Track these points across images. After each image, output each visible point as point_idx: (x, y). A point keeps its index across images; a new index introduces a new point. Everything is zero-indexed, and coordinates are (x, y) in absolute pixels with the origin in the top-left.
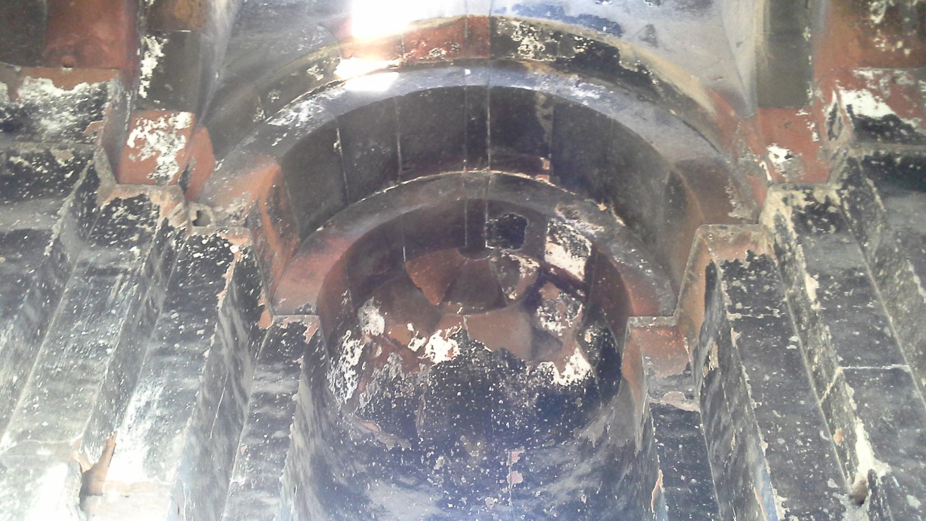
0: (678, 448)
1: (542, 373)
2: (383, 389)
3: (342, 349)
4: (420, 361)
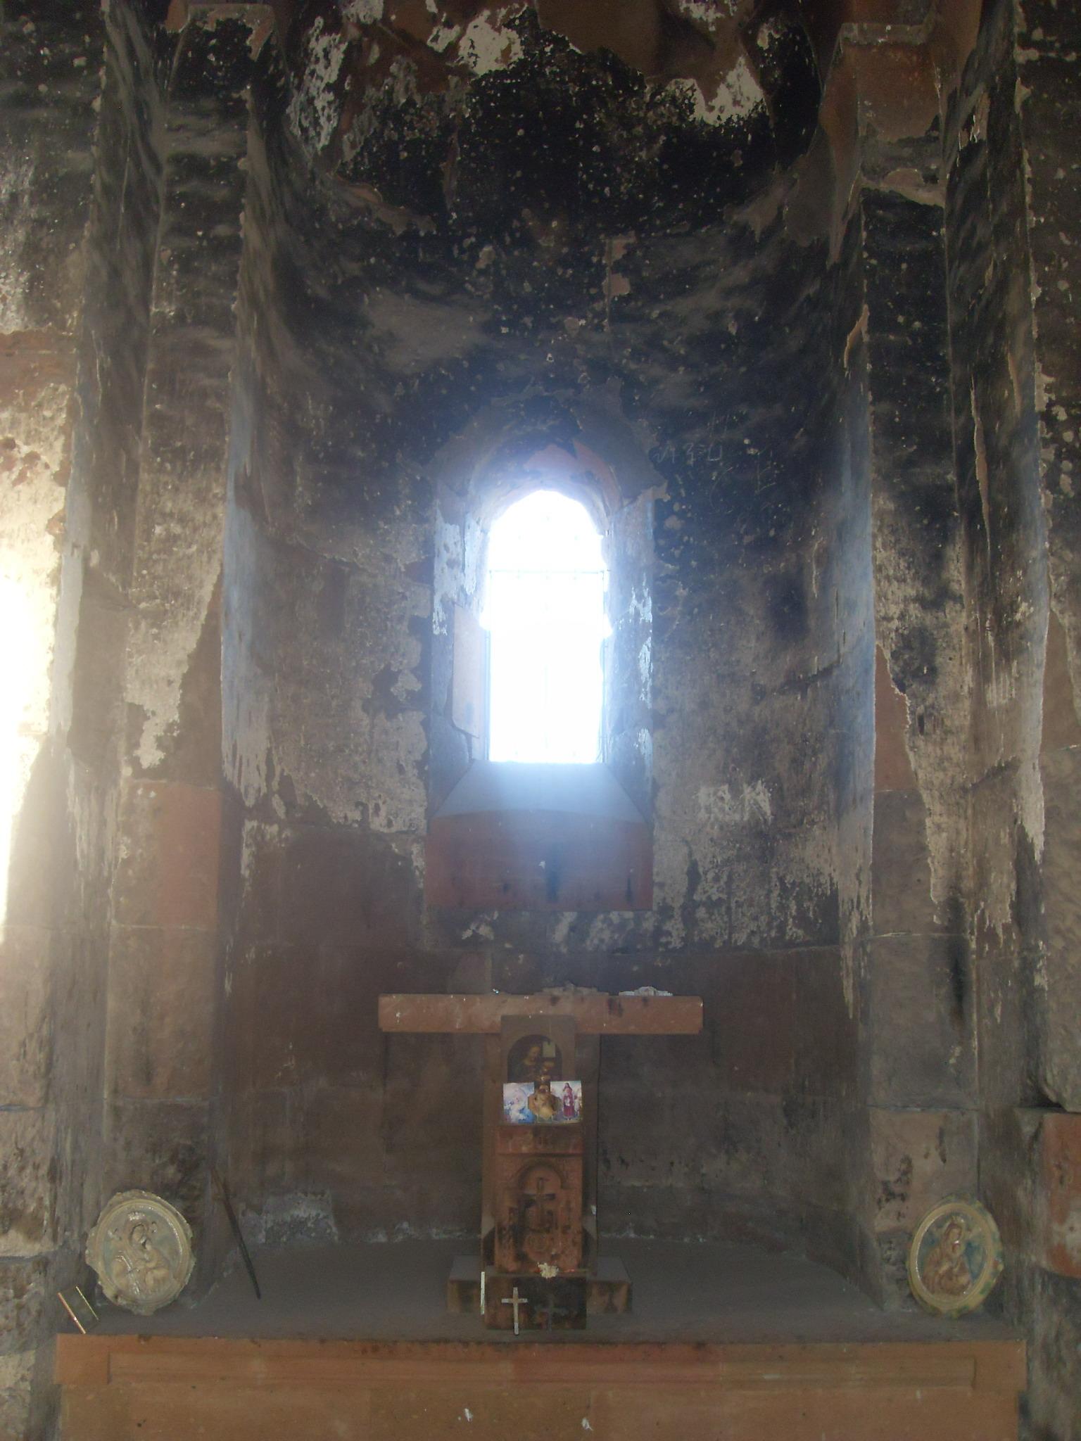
0: (900, 270)
1: (674, 99)
2: (384, 124)
3: (308, 54)
4: (450, 71)
